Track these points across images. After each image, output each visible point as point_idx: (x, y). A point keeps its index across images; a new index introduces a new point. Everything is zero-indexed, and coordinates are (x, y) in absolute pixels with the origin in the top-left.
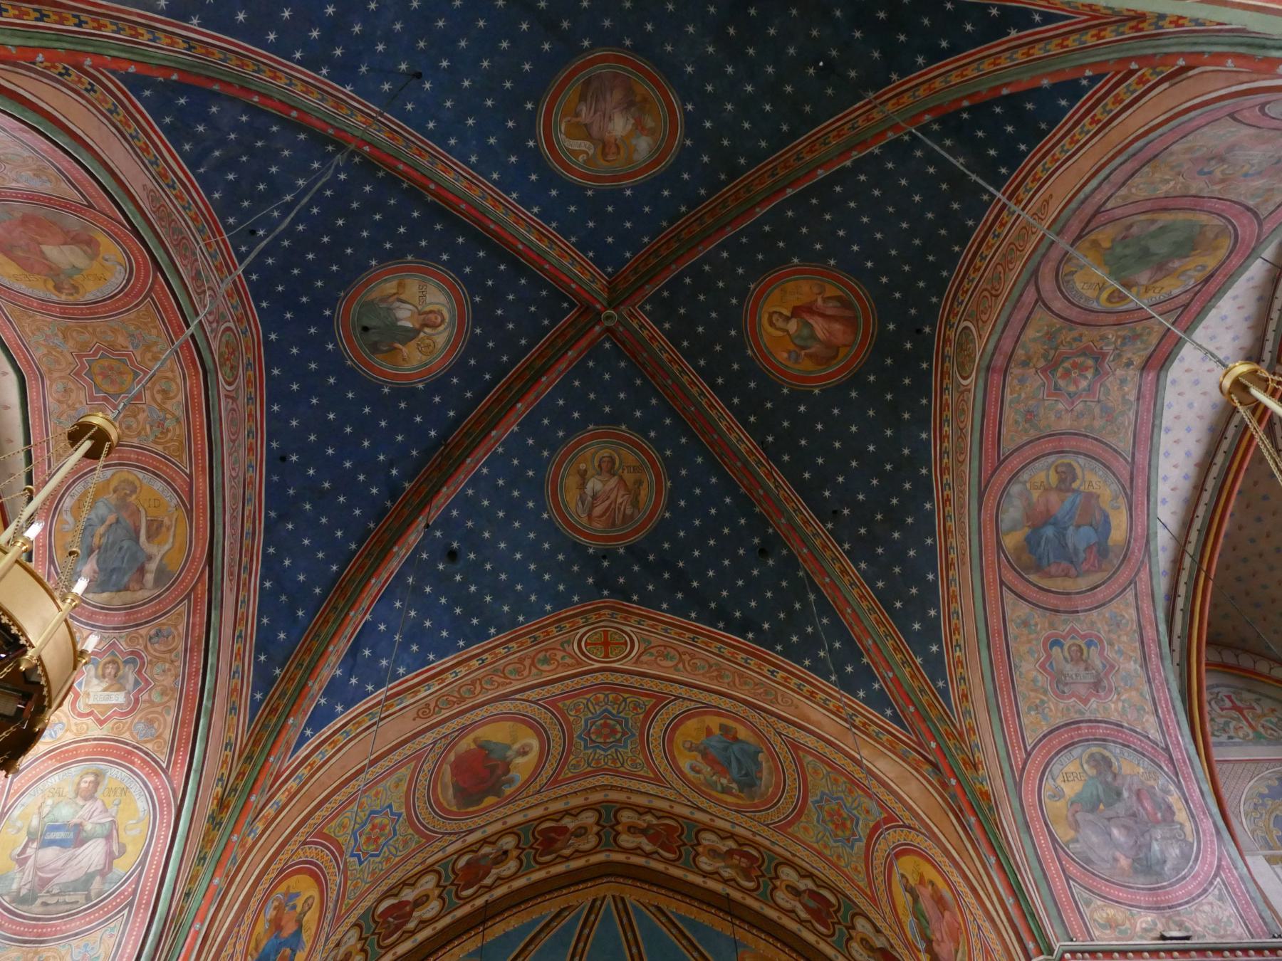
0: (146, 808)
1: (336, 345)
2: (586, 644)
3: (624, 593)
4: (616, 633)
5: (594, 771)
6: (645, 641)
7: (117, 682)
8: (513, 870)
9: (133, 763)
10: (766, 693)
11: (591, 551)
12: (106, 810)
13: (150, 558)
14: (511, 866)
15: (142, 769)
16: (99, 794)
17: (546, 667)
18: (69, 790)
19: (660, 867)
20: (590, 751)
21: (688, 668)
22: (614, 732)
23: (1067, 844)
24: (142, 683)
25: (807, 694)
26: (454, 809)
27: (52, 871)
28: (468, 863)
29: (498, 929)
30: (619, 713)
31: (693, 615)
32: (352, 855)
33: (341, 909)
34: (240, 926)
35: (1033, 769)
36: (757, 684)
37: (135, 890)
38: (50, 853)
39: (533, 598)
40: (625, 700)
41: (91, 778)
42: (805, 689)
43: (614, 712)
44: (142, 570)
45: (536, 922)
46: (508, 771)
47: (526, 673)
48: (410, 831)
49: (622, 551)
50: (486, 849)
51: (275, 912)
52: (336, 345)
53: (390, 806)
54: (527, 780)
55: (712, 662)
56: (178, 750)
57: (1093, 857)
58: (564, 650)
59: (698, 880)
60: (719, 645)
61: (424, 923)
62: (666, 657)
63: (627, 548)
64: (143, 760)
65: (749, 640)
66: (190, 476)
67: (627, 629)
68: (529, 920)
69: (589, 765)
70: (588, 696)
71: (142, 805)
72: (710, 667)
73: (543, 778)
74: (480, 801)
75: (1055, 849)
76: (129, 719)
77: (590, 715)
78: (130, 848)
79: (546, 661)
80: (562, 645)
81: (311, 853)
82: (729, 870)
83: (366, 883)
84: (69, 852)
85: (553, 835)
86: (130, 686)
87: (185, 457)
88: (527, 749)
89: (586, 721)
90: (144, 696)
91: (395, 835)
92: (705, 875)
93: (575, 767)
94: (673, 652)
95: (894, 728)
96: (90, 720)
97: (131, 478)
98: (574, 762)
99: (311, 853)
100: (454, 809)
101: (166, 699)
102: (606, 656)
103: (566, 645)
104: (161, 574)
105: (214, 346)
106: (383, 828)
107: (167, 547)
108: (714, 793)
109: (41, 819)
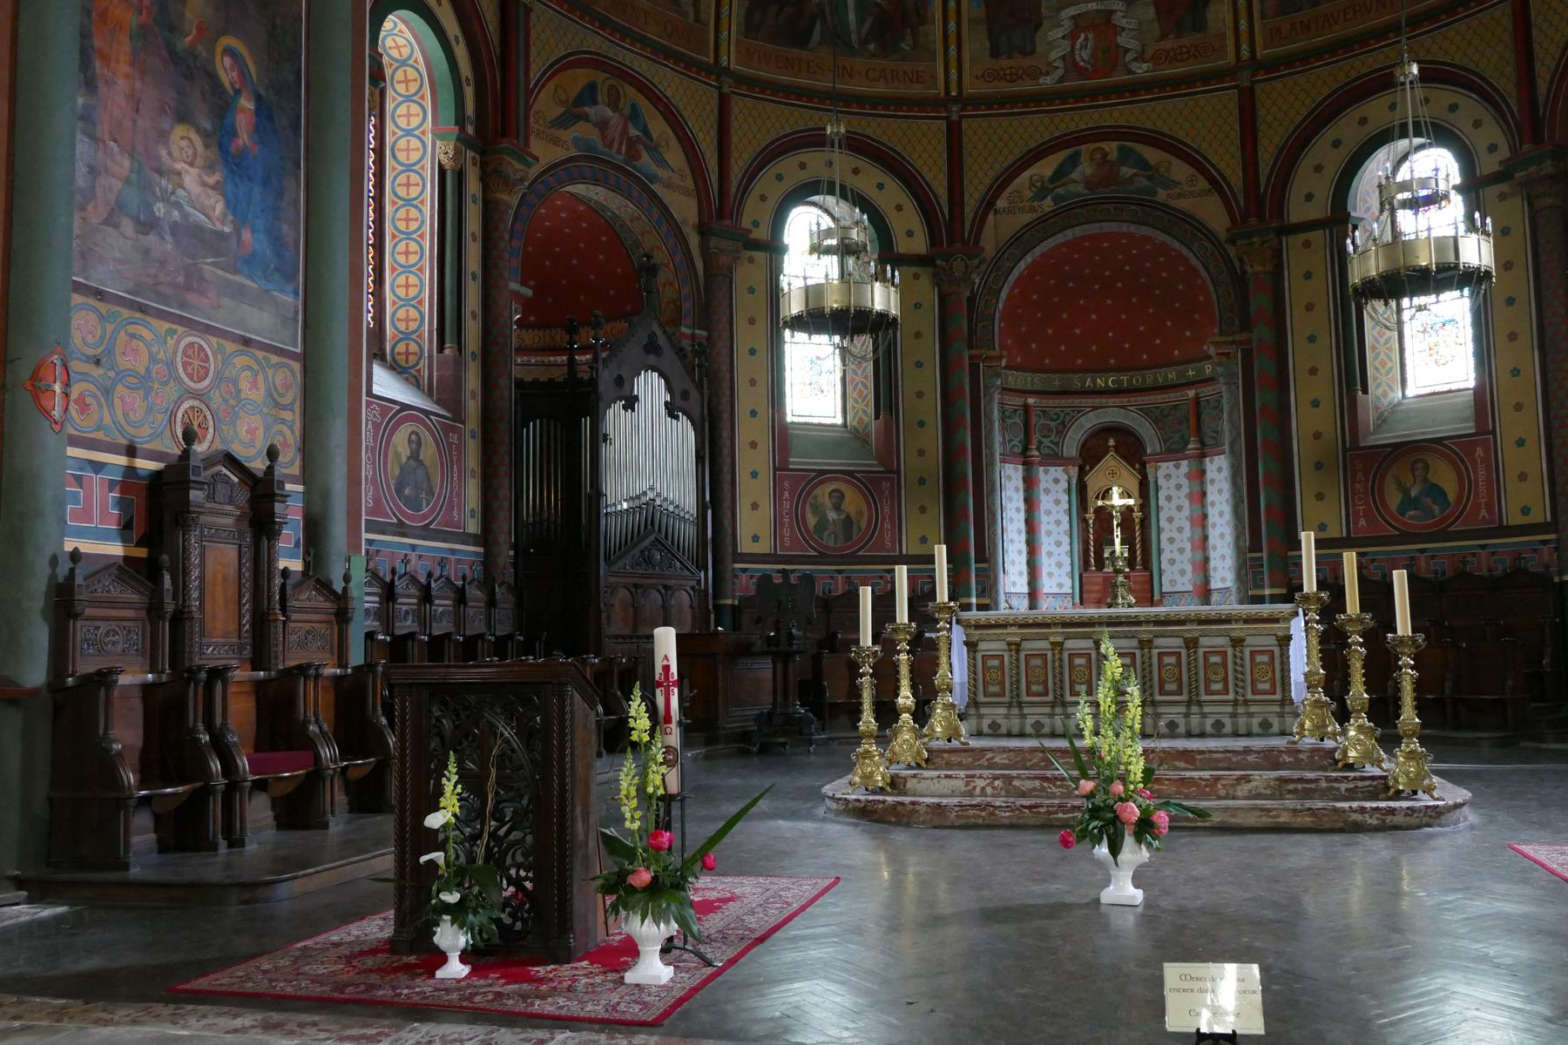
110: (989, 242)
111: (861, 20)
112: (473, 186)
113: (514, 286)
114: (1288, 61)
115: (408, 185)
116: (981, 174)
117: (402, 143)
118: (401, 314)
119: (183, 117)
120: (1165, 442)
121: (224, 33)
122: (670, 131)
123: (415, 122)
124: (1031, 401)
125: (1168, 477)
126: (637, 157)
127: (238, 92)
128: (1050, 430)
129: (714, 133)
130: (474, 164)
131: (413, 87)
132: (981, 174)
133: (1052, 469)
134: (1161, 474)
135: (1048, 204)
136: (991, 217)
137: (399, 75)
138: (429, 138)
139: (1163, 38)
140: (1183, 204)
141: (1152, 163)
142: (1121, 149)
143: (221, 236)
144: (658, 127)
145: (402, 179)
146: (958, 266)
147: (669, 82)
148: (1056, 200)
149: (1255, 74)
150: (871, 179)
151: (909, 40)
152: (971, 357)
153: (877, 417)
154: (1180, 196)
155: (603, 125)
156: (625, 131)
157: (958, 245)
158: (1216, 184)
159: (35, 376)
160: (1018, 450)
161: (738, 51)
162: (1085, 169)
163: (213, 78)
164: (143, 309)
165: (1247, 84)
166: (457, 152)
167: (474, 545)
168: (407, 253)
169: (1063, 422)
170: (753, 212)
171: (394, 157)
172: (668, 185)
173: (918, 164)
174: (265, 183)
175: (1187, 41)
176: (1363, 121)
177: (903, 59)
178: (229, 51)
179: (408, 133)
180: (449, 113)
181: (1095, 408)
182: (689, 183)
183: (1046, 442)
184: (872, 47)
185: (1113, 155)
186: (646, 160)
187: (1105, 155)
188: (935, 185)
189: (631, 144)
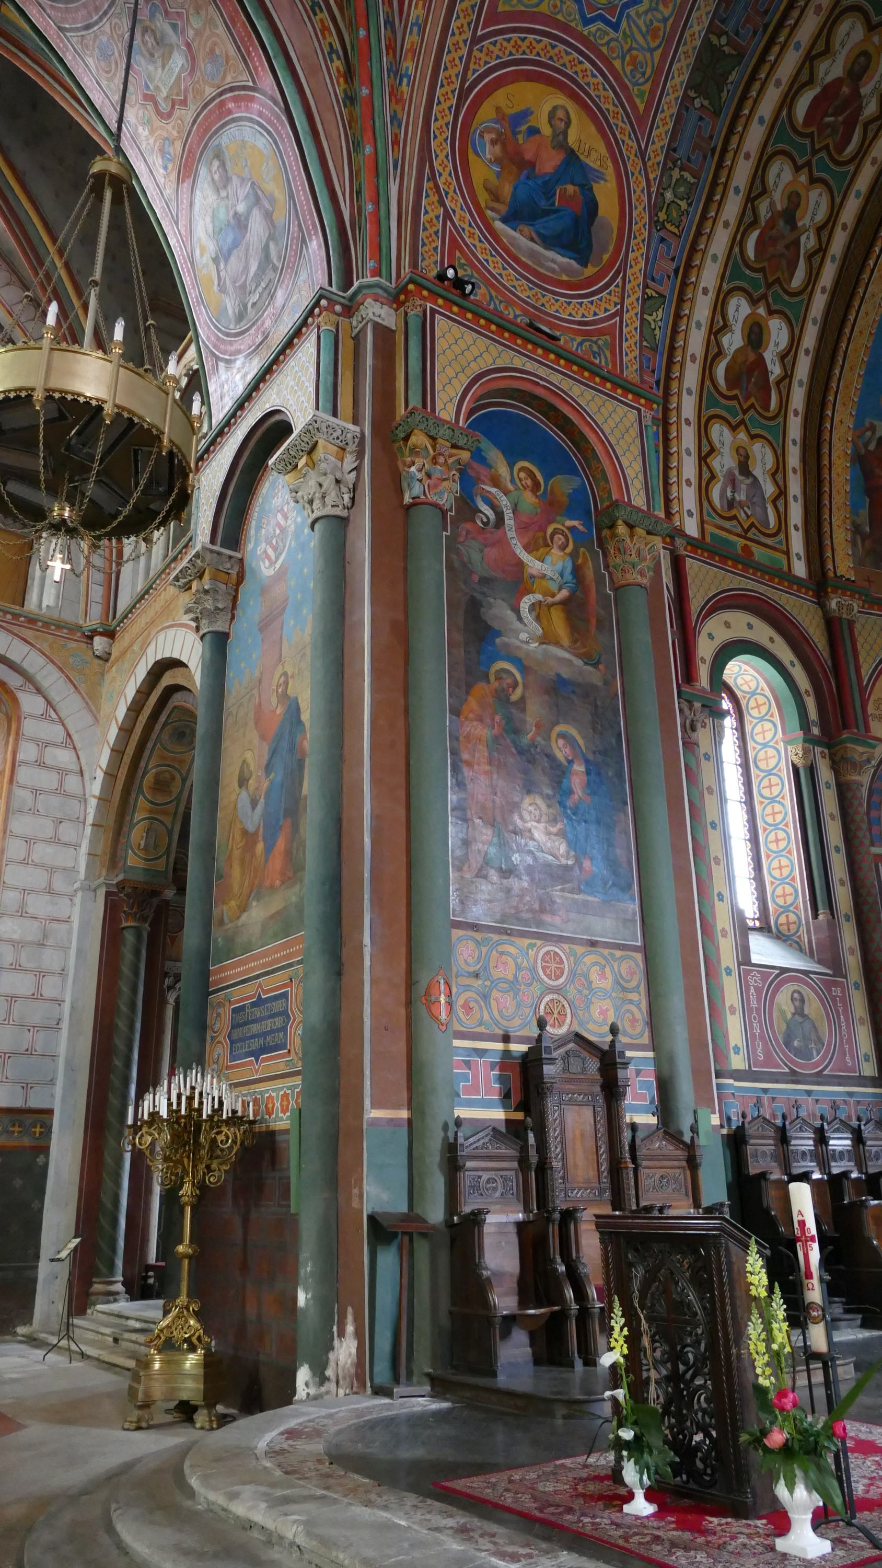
0: (265, 141)
12: (243, 180)
32: (587, 22)
34: (433, 178)
37: (300, 225)
51: (498, 149)
56: (249, 53)
64: (235, 99)
83: (652, 51)
84: (242, 248)
96: (177, 113)
112: (825, 774)
115: (770, 786)
117: (761, 755)
118: (779, 891)
121: (557, 723)
123: (769, 736)
127: (570, 762)
130: (824, 757)
131: (764, 710)
137: (752, 703)
138: (781, 746)
143: (567, 868)
145: (765, 782)
159: (428, 993)
163: (551, 757)
164: (505, 932)
166: (806, 752)
167: (875, 1087)
168: (777, 841)
171: (757, 767)
174: (598, 822)
178: (562, 736)
179: (765, 745)
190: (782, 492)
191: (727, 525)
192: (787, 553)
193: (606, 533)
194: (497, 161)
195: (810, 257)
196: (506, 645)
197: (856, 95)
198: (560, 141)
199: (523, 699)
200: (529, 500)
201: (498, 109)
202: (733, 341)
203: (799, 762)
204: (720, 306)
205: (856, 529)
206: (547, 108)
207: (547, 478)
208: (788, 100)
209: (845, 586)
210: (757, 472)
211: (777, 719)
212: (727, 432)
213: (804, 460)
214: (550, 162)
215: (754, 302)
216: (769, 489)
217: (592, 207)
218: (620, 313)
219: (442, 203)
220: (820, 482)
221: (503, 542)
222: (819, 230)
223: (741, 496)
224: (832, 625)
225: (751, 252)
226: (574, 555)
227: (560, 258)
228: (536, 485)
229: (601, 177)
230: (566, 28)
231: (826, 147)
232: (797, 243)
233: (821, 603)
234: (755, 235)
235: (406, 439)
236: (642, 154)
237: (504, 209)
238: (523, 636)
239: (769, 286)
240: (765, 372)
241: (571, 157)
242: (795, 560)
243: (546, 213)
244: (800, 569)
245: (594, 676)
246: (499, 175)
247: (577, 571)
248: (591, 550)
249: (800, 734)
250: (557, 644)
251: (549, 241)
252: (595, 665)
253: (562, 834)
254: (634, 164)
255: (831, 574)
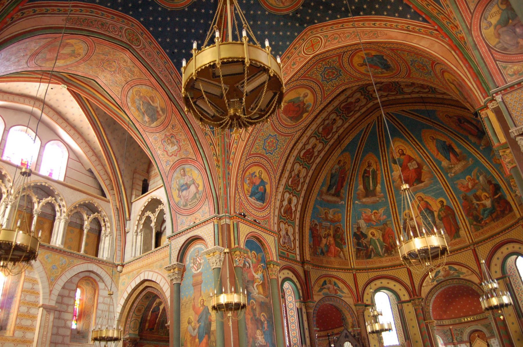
1: (161, 7)
2: (306, 49)
3: (311, 22)
4: (315, 39)
5: (337, 87)
6: (325, 36)
7: (173, 144)
8: (341, 122)
9: (189, 162)
10: (374, 34)
11: (291, 14)
13: (157, 107)
14: (339, 122)
15: (191, 163)
16: (186, 174)
17: (295, 66)
18: (180, 176)
19: (393, 98)
20: (330, 83)
21: (343, 39)
22: (334, 73)
23: (495, 47)
24: (178, 141)
25: (389, 26)
26: (294, 124)
27: (187, 196)
28: (323, 129)
29: (347, 142)
30: (330, 66)
31: (339, 16)
32: (267, 154)
33: (274, 168)
34: (238, 190)
35: (475, 21)
36: (369, 33)
38: (184, 193)
39: (281, 43)
40: (328, 62)
41: (182, 171)
42: (388, 25)
43: (328, 67)
44: (158, 112)
45: (359, 134)
46: (304, 104)
47: (289, 72)
48: (283, 137)
49: (301, 8)
50: (326, 122)
52: (161, 7)
53: (270, 135)
54: (314, 102)
55: (351, 32)
57: (506, 46)
58: (299, 56)
59: (409, 96)
60: (352, 23)
61: (320, 152)
62: (334, 39)
63: (303, 5)
65: (362, 15)
66: (149, 80)
67: (318, 35)
68: (359, 132)
69: (333, 86)
70: (315, 67)
71: (196, 172)
72: (351, 34)
73: (319, 99)
74: (302, 117)
75: (490, 51)
76: (181, 152)
77: (321, 72)
78: (200, 184)
79: (294, 64)
80: (298, 55)
81: (251, 160)
82: (416, 89)
83: (278, 158)
84: (188, 190)
85: (348, 106)
86: (176, 143)
87: (144, 76)
88: (306, 94)
89: (321, 75)
90: (181, 144)
91: (278, 141)
92: (410, 94)
93: (329, 89)
94: (336, 36)
95: (425, 25)
96: (173, 156)
97: (137, 89)
98: (326, 89)
99: (251, 160)
100: (294, 124)
101: (186, 142)
102: (314, 51)
103: (299, 54)
104: (162, 109)
105: (124, 40)
106: (272, 141)
107: (158, 102)
108: (380, 75)
109: (178, 185)
110: (423, 295)
111: (382, 250)
112: (304, 310)
113: (315, 329)
114: (481, 242)
116: (417, 279)
117: (289, 304)
118: (294, 339)
119: (258, 329)
120: (490, 333)
121: (261, 313)
122: (343, 285)
123: (291, 300)
124: (451, 327)
125: (494, 343)
126: (337, 293)
128: (459, 334)
129: (353, 283)
131: (290, 293)
132: (417, 279)
133: (462, 345)
134: (492, 342)
135: (435, 283)
136: (422, 288)
137: (287, 291)
139: (451, 240)
140: (467, 278)
141: (457, 269)
142: (449, 267)
144: (341, 285)
146: (417, 301)
147: (341, 275)
148: (437, 281)
149: (474, 245)
150: (392, 284)
151: (394, 251)
152: (425, 323)
153: (406, 341)
154: (466, 276)
155: (329, 289)
156: (334, 288)
157: (416, 297)
158: (473, 272)
160: (451, 341)
161: (356, 263)
162: (442, 273)
163: (261, 320)
165: (473, 248)
168: (293, 327)
169: (462, 332)
170: (366, 299)
172: (345, 297)
173: (402, 279)
175: (457, 240)
176: (502, 253)
177: (394, 256)
178: (263, 315)
179: (290, 302)
180: (297, 297)
181: (469, 326)
182: (350, 295)
183: (458, 337)
184: (386, 255)
185: (448, 269)
186: (339, 293)
187: (446, 269)
188: (407, 283)
189: (335, 290)
190: (295, 239)
191: (283, 248)
192: (296, 254)
193: (268, 266)
194: (249, 183)
195: (302, 184)
196: (252, 296)
197: (313, 151)
198: (260, 178)
199: (256, 308)
200: (254, 260)
201: (249, 173)
202: (285, 203)
203: (298, 307)
204: (283, 196)
205: (310, 246)
206: (258, 171)
207: (257, 254)
208: (299, 152)
209: (308, 262)
210: (290, 234)
211: (293, 296)
212: (283, 225)
213: (299, 230)
214: (258, 182)
215: (290, 194)
216: (292, 238)
217: (265, 190)
218: (270, 213)
219: (239, 195)
220: (303, 236)
221: (250, 272)
222: (304, 177)
223: (286, 241)
224: (306, 273)
225: (290, 183)
226: (263, 272)
227: (259, 203)
228: (256, 256)
229: (267, 183)
230: (263, 155)
231: (306, 161)
232: (299, 181)
233: (303, 267)
234: (291, 179)
235: (235, 252)
236: (275, 177)
237: (250, 194)
238: (255, 293)
239: (293, 190)
240: (292, 210)
241: (262, 180)
242: (297, 256)
243: (257, 193)
244: (298, 258)
245: (267, 300)
246: (249, 186)
247: (263, 276)
248: (266, 271)
249: (299, 300)
250: (261, 294)
251: (258, 199)
252: (267, 298)
253: (264, 338)
254: (273, 180)
255: (305, 260)
